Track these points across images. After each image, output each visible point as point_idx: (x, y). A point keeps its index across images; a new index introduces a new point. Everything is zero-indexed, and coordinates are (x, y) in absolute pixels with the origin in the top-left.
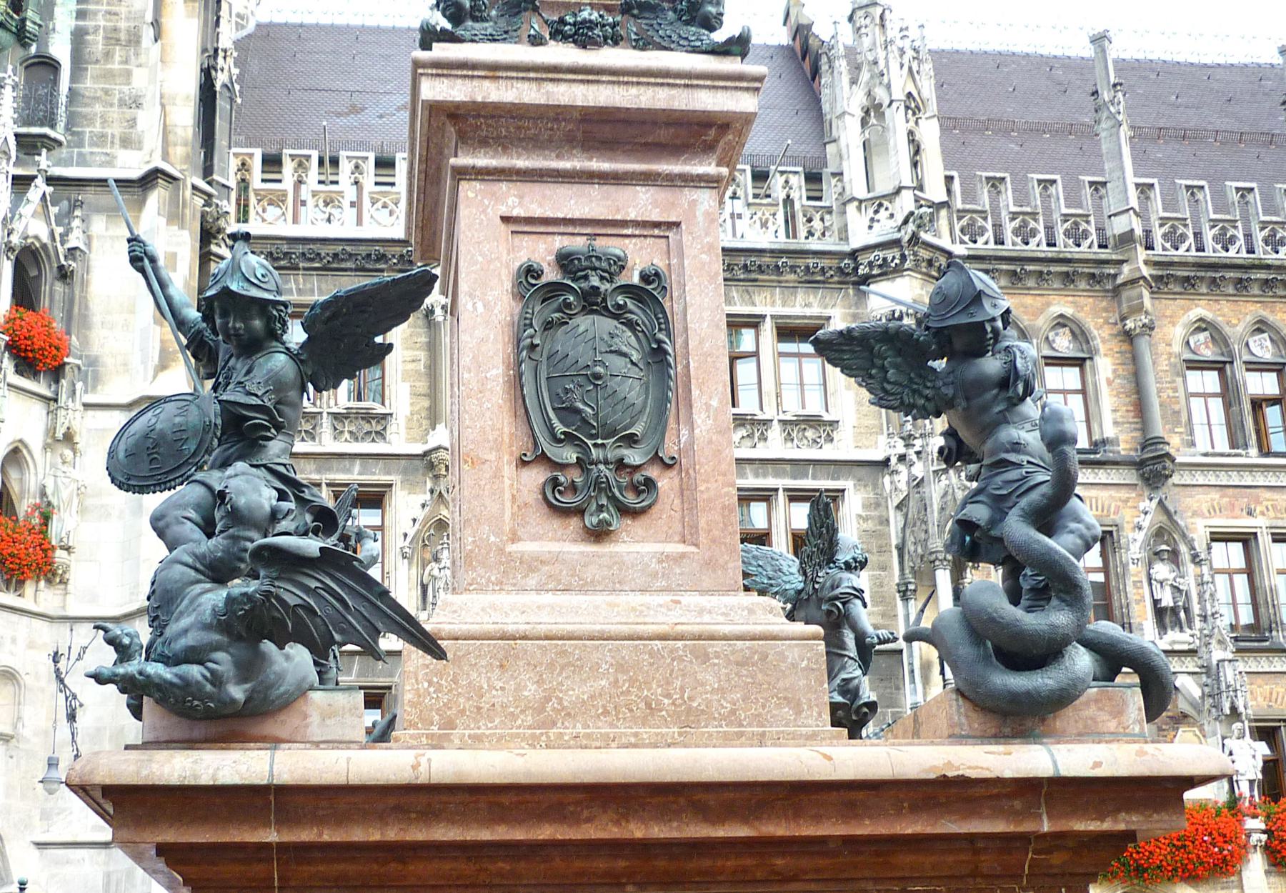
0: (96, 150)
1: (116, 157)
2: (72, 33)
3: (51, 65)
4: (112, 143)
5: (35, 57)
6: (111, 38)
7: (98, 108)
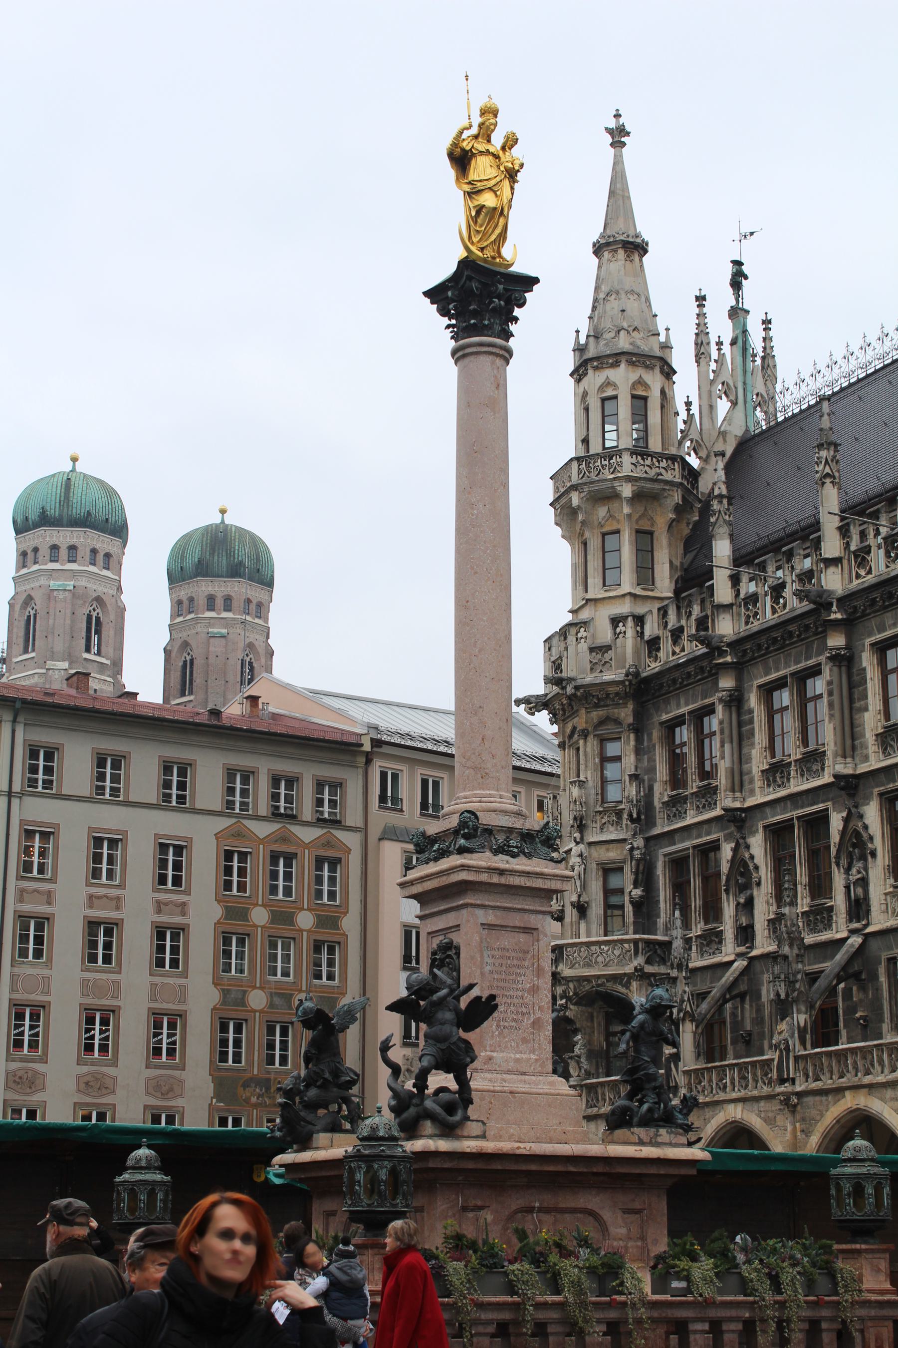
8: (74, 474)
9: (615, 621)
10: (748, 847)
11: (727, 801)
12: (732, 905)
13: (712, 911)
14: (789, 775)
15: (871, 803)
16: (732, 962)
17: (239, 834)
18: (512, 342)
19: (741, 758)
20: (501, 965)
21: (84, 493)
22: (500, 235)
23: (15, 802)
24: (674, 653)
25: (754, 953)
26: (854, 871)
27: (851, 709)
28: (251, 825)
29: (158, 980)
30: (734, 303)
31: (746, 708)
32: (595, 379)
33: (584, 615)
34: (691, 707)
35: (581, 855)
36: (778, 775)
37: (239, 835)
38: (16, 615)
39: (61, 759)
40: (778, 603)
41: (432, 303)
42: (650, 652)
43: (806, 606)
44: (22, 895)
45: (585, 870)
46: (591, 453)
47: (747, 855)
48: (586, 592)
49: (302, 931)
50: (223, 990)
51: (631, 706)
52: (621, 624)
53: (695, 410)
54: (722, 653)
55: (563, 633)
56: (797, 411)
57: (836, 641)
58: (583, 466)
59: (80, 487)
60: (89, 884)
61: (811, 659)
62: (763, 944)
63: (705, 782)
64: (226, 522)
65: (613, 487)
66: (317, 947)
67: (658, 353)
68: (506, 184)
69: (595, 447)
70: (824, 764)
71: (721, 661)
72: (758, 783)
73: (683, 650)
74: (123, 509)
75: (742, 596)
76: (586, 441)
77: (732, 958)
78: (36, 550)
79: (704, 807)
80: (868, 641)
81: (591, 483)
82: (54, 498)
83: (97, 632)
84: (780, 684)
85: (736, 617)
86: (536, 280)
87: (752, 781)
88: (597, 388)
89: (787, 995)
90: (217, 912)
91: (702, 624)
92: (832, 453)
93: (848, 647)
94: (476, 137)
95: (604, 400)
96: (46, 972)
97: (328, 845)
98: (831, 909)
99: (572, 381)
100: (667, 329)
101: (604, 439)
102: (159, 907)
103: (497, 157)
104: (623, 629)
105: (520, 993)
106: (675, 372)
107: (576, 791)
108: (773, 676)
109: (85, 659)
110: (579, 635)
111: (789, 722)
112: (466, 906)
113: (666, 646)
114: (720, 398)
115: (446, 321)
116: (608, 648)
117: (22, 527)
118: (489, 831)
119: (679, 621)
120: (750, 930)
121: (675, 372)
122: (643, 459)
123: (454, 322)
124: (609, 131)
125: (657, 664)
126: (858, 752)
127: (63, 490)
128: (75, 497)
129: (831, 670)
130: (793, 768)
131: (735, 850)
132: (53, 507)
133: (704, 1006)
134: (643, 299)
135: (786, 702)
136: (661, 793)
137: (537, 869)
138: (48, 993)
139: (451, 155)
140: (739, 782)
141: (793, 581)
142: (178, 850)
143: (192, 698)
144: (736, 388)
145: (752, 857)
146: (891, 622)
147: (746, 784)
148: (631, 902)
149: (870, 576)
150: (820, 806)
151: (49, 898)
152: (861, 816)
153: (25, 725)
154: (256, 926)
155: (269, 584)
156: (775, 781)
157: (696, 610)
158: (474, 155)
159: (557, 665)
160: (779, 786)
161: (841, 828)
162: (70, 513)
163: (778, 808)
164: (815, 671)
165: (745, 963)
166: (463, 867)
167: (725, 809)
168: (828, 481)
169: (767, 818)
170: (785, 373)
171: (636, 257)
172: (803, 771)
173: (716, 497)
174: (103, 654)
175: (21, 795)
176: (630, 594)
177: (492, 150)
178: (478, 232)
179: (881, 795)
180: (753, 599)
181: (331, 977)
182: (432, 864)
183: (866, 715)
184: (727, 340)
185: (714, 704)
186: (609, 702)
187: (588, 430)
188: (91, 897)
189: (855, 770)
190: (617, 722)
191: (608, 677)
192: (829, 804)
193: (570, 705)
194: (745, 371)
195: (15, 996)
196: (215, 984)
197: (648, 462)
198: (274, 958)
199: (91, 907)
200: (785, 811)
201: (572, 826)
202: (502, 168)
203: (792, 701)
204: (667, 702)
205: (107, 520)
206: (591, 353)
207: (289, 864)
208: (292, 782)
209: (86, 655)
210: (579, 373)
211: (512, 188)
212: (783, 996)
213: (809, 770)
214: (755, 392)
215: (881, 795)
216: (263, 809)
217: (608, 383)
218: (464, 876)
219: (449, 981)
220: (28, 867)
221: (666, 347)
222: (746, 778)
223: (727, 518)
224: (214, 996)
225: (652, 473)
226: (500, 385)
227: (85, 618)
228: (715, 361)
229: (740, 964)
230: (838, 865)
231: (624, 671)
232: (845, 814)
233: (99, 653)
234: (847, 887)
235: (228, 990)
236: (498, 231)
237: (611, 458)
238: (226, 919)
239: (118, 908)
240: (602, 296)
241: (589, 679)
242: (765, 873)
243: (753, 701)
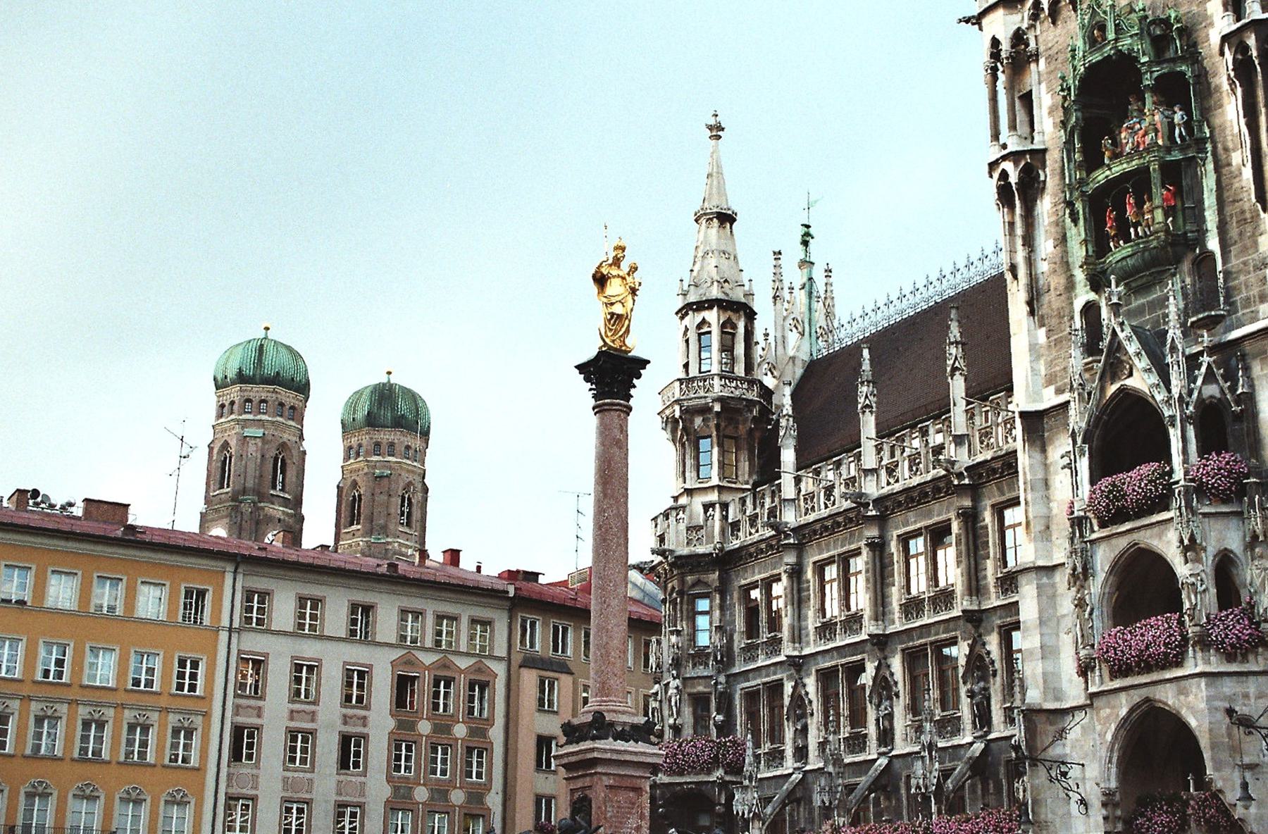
0: (1245, 311)
1: (1258, 312)
2: (1218, 228)
3: (1212, 254)
4: (1254, 302)
5: (1200, 254)
6: (1241, 220)
7: (1242, 278)
9: (707, 507)
10: (804, 686)
11: (788, 650)
12: (792, 729)
13: (776, 735)
14: (836, 631)
15: (896, 656)
16: (790, 775)
17: (409, 662)
18: (632, 402)
19: (799, 617)
20: (618, 812)
22: (625, 332)
23: (235, 636)
24: (750, 534)
25: (808, 768)
26: (883, 707)
27: (882, 584)
28: (421, 656)
29: (342, 778)
30: (803, 256)
31: (804, 578)
32: (693, 319)
33: (683, 500)
34: (763, 576)
35: (677, 688)
36: (827, 632)
37: (410, 663)
39: (271, 601)
40: (830, 500)
41: (580, 373)
42: (732, 532)
43: (847, 504)
44: (238, 710)
45: (680, 699)
46: (690, 376)
47: (803, 692)
48: (685, 483)
49: (457, 739)
50: (395, 787)
52: (711, 509)
53: (771, 339)
54: (787, 537)
55: (666, 515)
56: (849, 343)
57: (873, 532)
58: (683, 386)
60: (291, 701)
61: (853, 543)
62: (814, 763)
63: (773, 634)
64: (392, 382)
66: (470, 750)
67: (743, 300)
68: (630, 298)
69: (693, 372)
70: (862, 624)
71: (786, 542)
72: (812, 638)
73: (757, 531)
75: (803, 492)
76: (686, 366)
77: (791, 771)
78: (232, 403)
79: (771, 653)
80: (895, 533)
81: (690, 399)
83: (283, 472)
84: (830, 561)
85: (797, 508)
86: (648, 362)
87: (807, 635)
88: (695, 325)
89: (831, 803)
90: (391, 723)
91: (772, 513)
92: (871, 388)
93: (881, 537)
94: (610, 265)
95: (700, 335)
96: (255, 771)
97: (479, 671)
98: (866, 736)
99: (677, 318)
101: (700, 364)
102: (346, 719)
103: (624, 278)
104: (713, 513)
105: (629, 830)
106: (756, 314)
107: (674, 639)
108: (825, 555)
109: (272, 495)
110: (678, 517)
111: (833, 592)
112: (596, 773)
113: (745, 527)
114: (791, 330)
115: (589, 385)
116: (702, 527)
117: (220, 385)
118: (612, 724)
119: (755, 509)
120: (805, 750)
121: (756, 314)
122: (730, 382)
123: (594, 387)
124: (711, 128)
125: (738, 541)
126: (887, 617)
129: (868, 554)
130: (838, 626)
131: (795, 688)
133: (769, 810)
134: (732, 258)
135: (835, 575)
136: (739, 642)
137: (642, 750)
138: (256, 788)
139: (594, 277)
140: (798, 636)
141: (841, 484)
142: (361, 675)
143: (359, 527)
144: (803, 323)
145: (807, 694)
146: (913, 520)
147: (803, 637)
148: (714, 725)
149: (897, 485)
150: (859, 657)
151: (259, 712)
152: (889, 666)
153: (244, 574)
154: (422, 736)
155: (426, 434)
156: (825, 636)
157: (768, 500)
158: (609, 278)
159: (662, 539)
160: (828, 640)
161: (873, 675)
163: (828, 656)
164: (857, 553)
165: (801, 776)
166: (593, 750)
167: (786, 656)
168: (867, 410)
169: (818, 664)
170: (842, 313)
171: (728, 225)
172: (846, 629)
173: (785, 416)
174: (287, 489)
175: (239, 631)
176: (718, 486)
177: (621, 274)
178: (611, 330)
179: (903, 650)
180: (811, 496)
181: (479, 775)
182: (574, 745)
183: (893, 588)
184: (797, 286)
185: (780, 574)
186: (700, 569)
187: (688, 357)
188: (292, 711)
189: (884, 630)
190: (707, 584)
191: (701, 550)
192: (865, 655)
193: (671, 570)
194: (810, 309)
195: (230, 791)
196: (388, 782)
197: (734, 385)
198: (434, 760)
199: (292, 719)
200: (832, 658)
201: (671, 665)
202: (628, 287)
203: (838, 575)
204: (745, 570)
205: (293, 379)
206: (692, 298)
207: (447, 686)
208: (453, 618)
209: (272, 492)
210: (683, 312)
211: (634, 301)
212: (827, 804)
213: (851, 629)
214: (818, 326)
215: (903, 650)
216: (429, 643)
217: (704, 322)
218: (596, 755)
219: (583, 823)
220: (242, 686)
221: (749, 295)
222: (803, 632)
223: (792, 432)
224: (387, 791)
225: (737, 393)
226: (623, 430)
227: (272, 460)
228: (788, 302)
229: (797, 777)
230: (871, 702)
231: (712, 545)
232: (876, 664)
233: (283, 490)
234: (877, 720)
235: (399, 787)
236: (623, 329)
237: (705, 381)
238: (398, 729)
239: (313, 721)
240: (700, 254)
241: (685, 551)
242: (816, 706)
243: (809, 574)
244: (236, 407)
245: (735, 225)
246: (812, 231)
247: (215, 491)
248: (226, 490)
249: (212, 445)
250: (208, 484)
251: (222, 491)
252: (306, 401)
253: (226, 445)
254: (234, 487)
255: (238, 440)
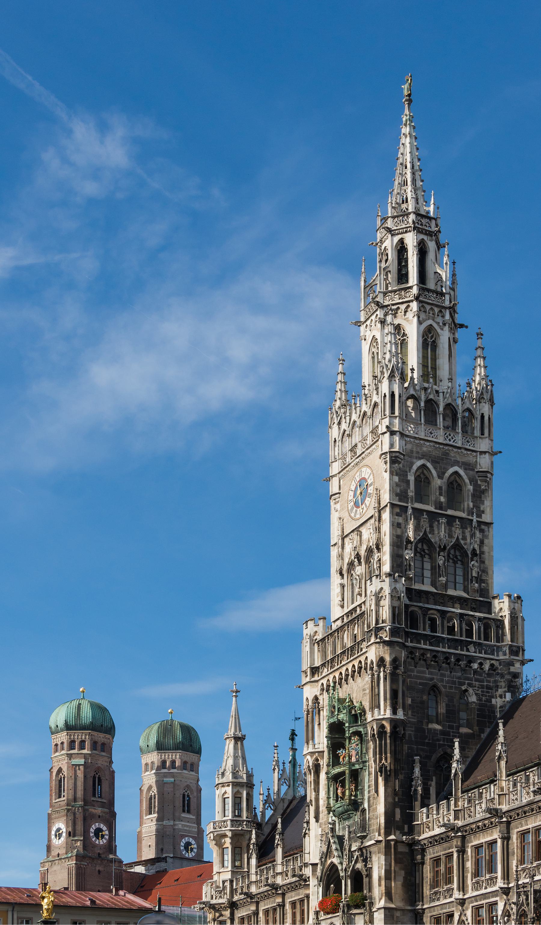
8: (83, 700)
9: (224, 882)
21: (88, 711)
38: (54, 778)
51: (229, 910)
59: (86, 708)
65: (225, 833)
74: (111, 719)
82: (71, 715)
100: (252, 769)
127: (76, 710)
128: (83, 714)
132: (71, 720)
162: (81, 723)
205: (102, 725)
227: (92, 779)
243: (261, 914)
244: (65, 745)
245: (244, 741)
246: (296, 733)
247: (55, 799)
248: (62, 799)
249: (52, 770)
250: (51, 795)
251: (60, 799)
252: (113, 738)
253: (60, 770)
254: (68, 796)
255: (68, 767)
